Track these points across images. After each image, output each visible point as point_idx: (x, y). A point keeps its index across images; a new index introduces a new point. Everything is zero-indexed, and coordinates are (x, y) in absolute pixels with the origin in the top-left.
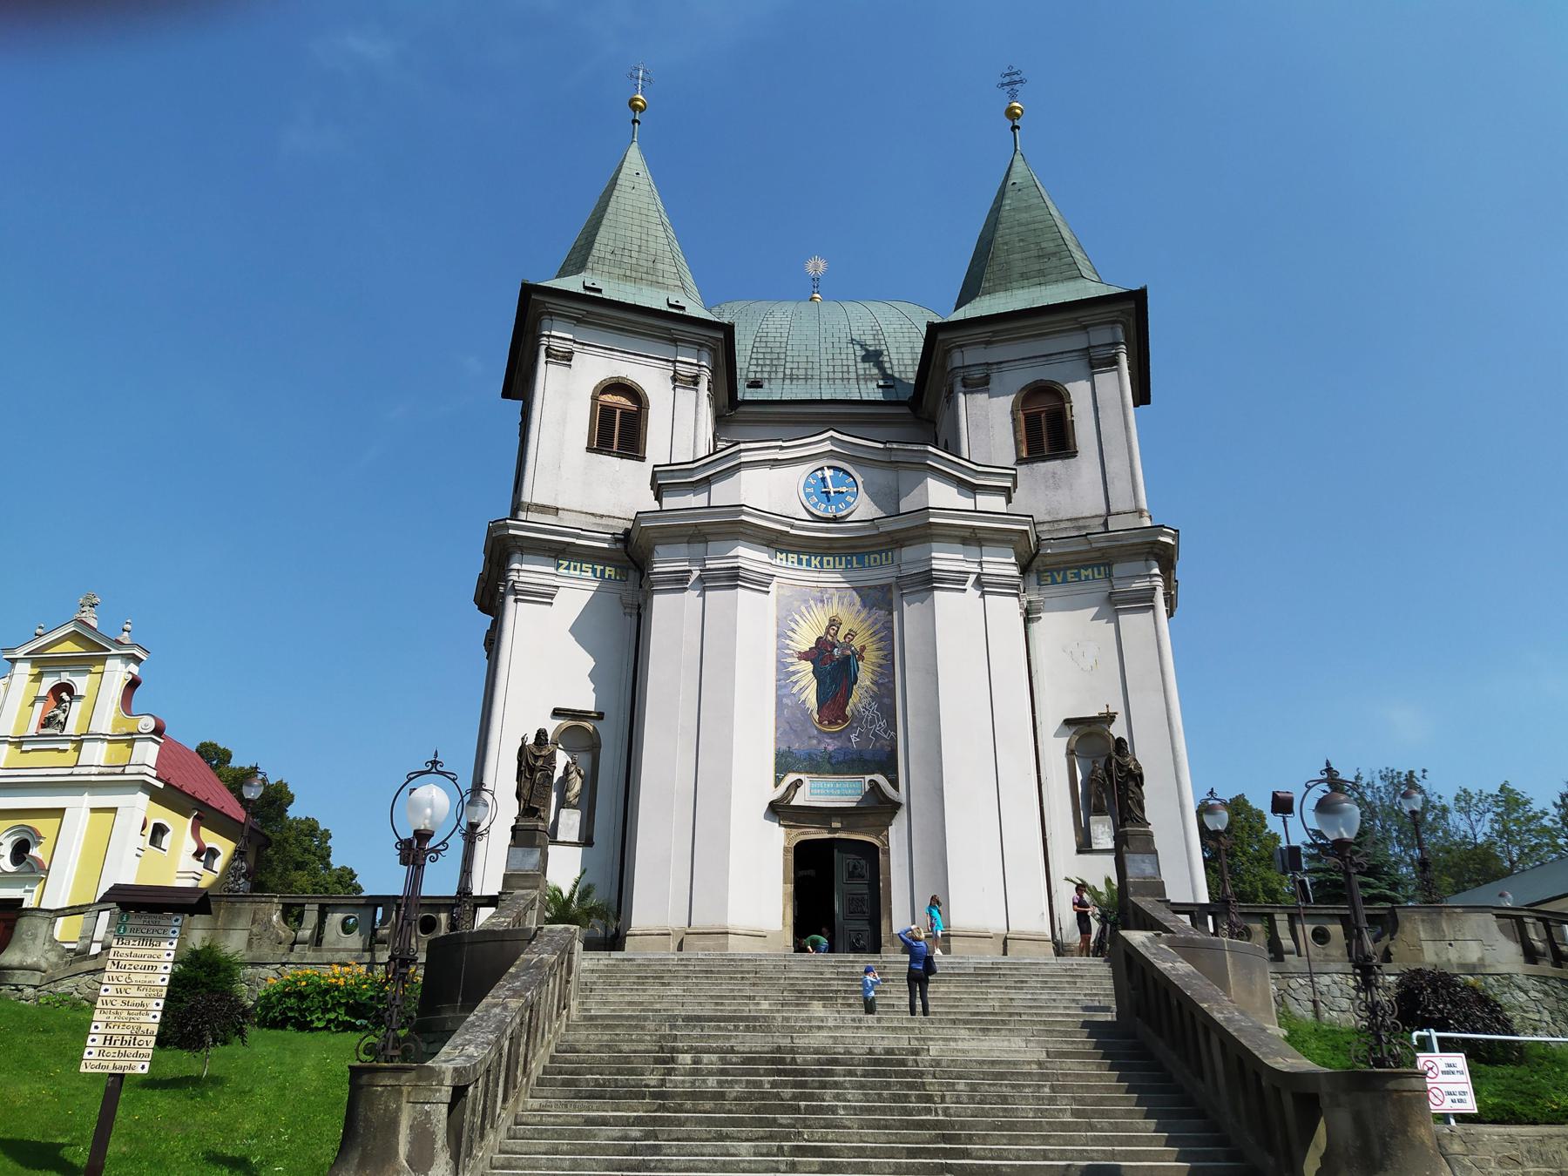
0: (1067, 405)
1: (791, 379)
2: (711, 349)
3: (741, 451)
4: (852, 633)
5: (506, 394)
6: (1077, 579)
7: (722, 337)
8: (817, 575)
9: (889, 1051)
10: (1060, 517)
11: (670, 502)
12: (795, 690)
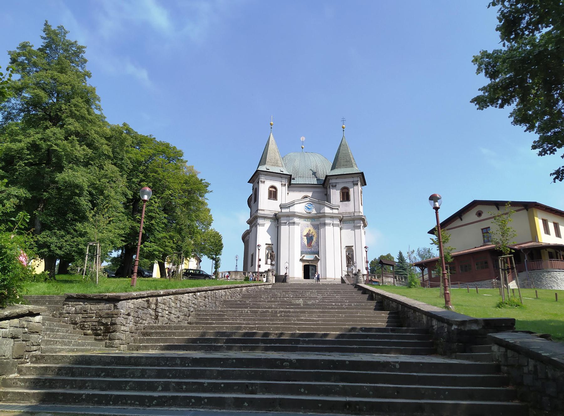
11: (284, 211)
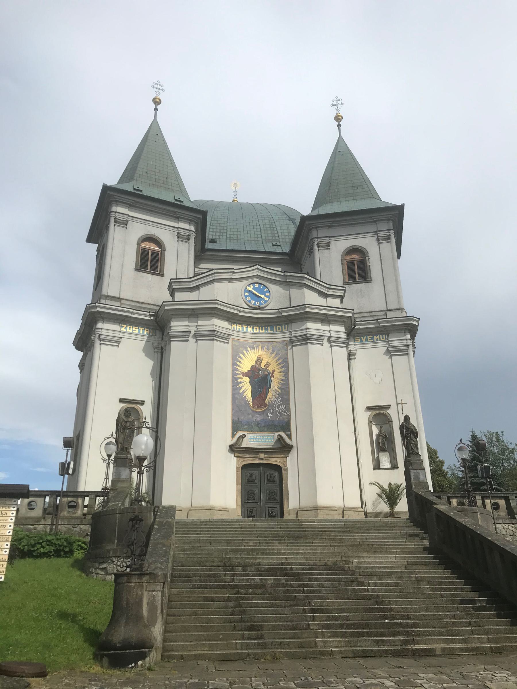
0: (367, 258)
1: (230, 239)
2: (196, 223)
3: (214, 273)
4: (268, 364)
5: (90, 239)
6: (372, 340)
7: (201, 217)
8: (251, 335)
9: (335, 563)
10: (364, 311)
11: (179, 296)
12: (241, 391)
